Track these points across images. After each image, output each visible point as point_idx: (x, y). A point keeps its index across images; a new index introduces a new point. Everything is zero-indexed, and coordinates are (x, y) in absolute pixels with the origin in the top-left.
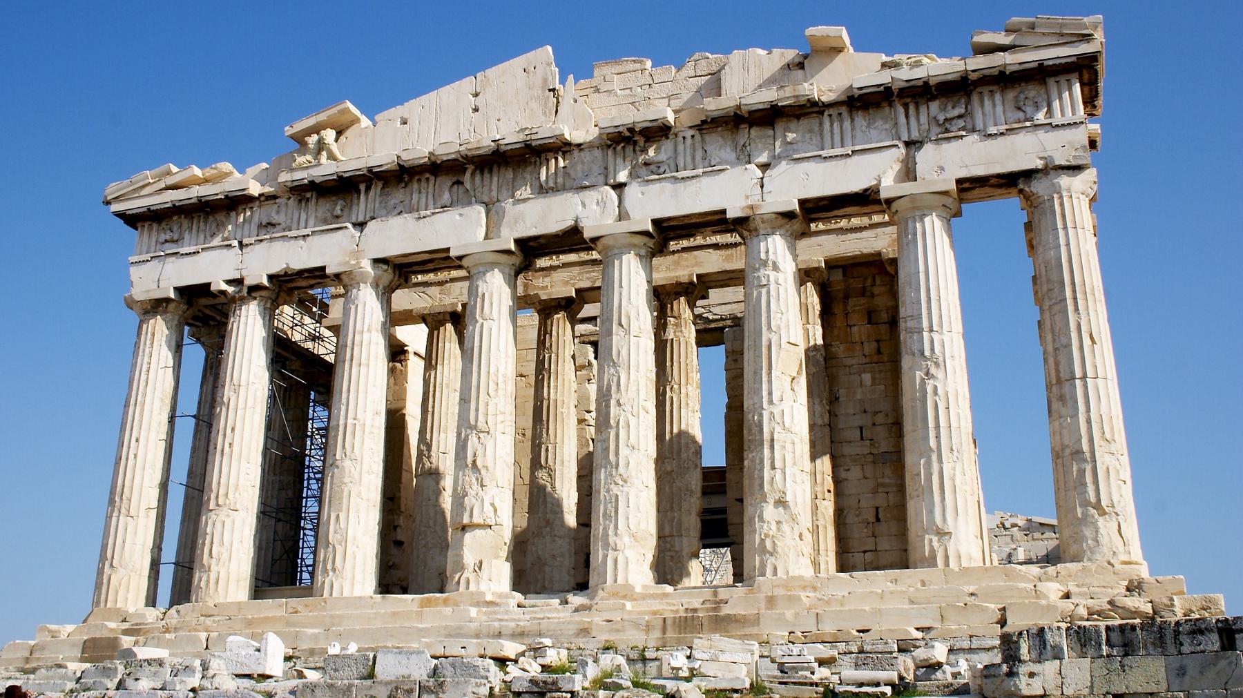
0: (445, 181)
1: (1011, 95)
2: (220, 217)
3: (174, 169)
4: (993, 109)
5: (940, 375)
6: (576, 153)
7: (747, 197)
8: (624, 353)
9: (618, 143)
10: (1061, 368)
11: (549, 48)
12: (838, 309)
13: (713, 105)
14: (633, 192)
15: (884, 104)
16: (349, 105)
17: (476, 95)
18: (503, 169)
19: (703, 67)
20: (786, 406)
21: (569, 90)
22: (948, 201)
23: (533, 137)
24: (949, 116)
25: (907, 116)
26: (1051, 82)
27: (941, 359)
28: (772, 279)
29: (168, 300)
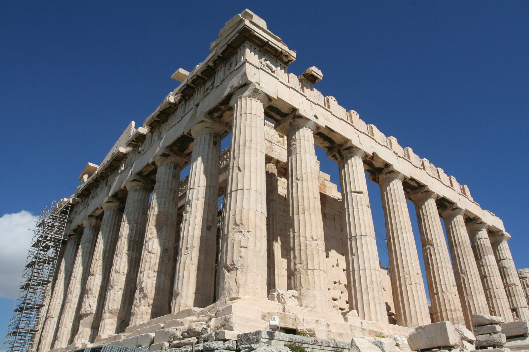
0: (105, 181)
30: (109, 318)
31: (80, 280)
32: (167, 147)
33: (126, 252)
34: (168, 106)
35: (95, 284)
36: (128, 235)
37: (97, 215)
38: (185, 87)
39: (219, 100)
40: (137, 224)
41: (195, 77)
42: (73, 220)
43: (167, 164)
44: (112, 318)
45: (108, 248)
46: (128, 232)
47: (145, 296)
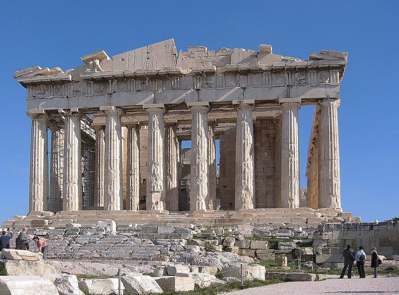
0: (139, 82)
2: (59, 87)
3: (40, 68)
5: (293, 156)
6: (184, 77)
7: (239, 98)
8: (200, 143)
10: (326, 156)
11: (173, 39)
13: (229, 67)
14: (203, 91)
15: (282, 72)
17: (148, 53)
19: (225, 53)
20: (249, 162)
21: (181, 55)
22: (298, 105)
26: (331, 71)
28: (246, 124)
29: (43, 114)
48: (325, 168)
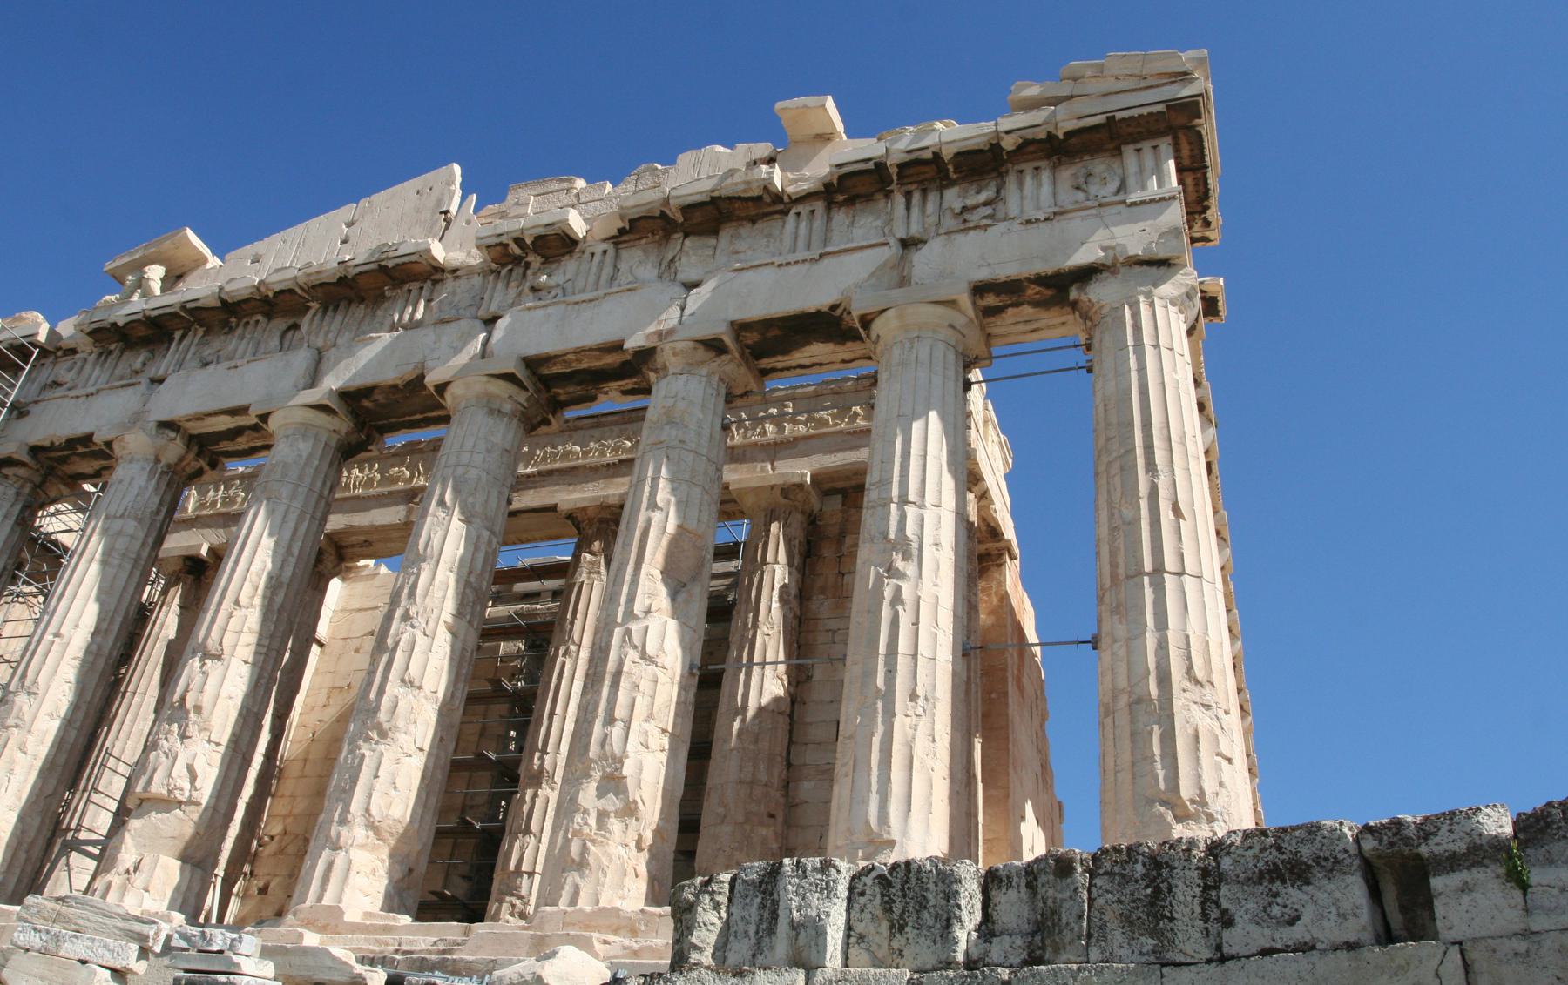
0: (280, 324)
1: (1066, 174)
4: (1034, 191)
5: (909, 569)
8: (436, 541)
9: (504, 265)
12: (828, 552)
15: (879, 196)
16: (189, 232)
18: (353, 306)
20: (654, 623)
23: (391, 254)
24: (970, 202)
25: (908, 208)
27: (915, 545)
30: (363, 846)
31: (81, 655)
32: (732, 323)
33: (450, 619)
34: (756, 193)
35: (223, 694)
36: (462, 559)
37: (195, 432)
38: (870, 165)
39: (1046, 268)
40: (493, 532)
41: (928, 155)
42: (34, 409)
43: (708, 376)
44: (374, 848)
45: (288, 572)
46: (461, 550)
47: (630, 811)
48: (1121, 630)
